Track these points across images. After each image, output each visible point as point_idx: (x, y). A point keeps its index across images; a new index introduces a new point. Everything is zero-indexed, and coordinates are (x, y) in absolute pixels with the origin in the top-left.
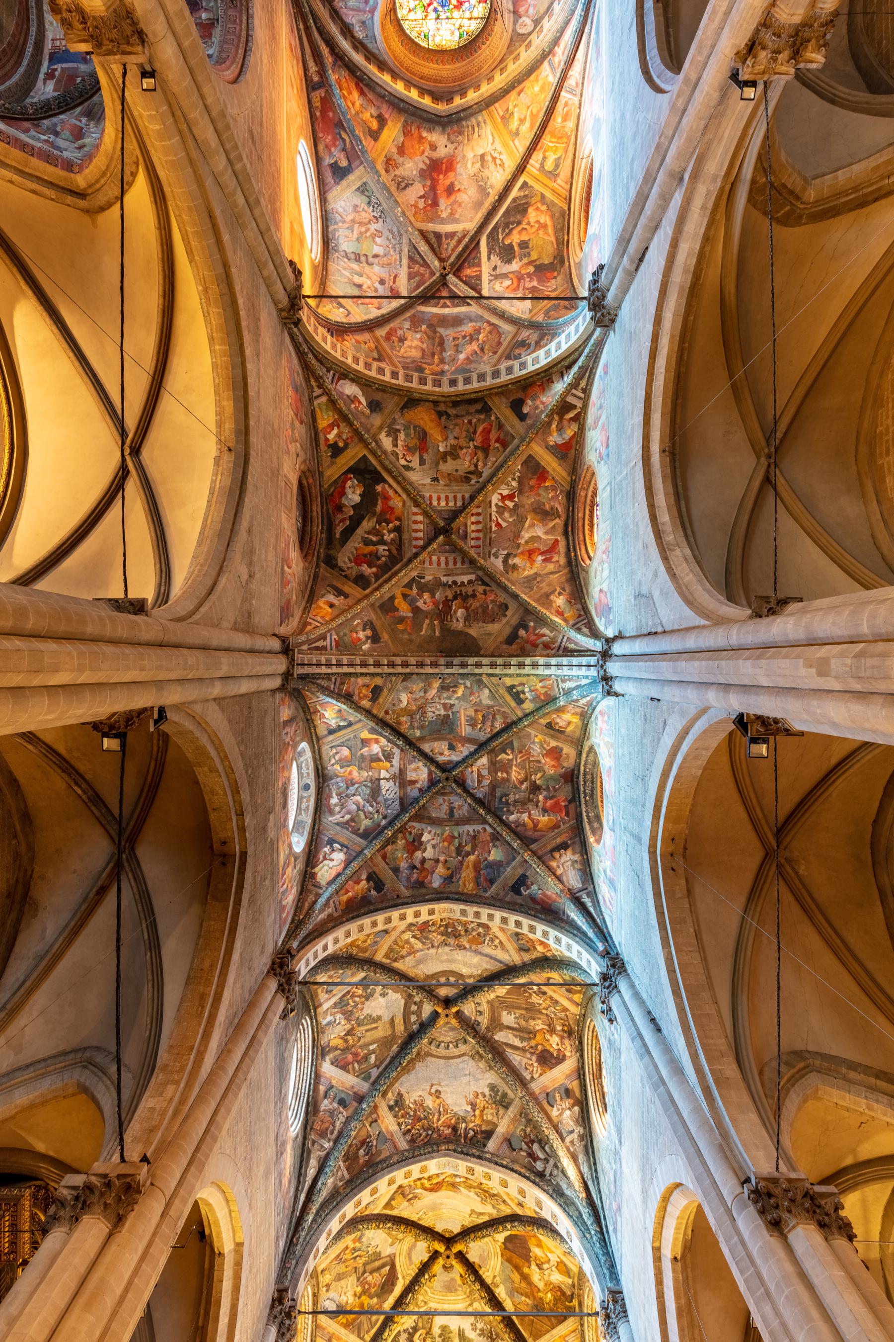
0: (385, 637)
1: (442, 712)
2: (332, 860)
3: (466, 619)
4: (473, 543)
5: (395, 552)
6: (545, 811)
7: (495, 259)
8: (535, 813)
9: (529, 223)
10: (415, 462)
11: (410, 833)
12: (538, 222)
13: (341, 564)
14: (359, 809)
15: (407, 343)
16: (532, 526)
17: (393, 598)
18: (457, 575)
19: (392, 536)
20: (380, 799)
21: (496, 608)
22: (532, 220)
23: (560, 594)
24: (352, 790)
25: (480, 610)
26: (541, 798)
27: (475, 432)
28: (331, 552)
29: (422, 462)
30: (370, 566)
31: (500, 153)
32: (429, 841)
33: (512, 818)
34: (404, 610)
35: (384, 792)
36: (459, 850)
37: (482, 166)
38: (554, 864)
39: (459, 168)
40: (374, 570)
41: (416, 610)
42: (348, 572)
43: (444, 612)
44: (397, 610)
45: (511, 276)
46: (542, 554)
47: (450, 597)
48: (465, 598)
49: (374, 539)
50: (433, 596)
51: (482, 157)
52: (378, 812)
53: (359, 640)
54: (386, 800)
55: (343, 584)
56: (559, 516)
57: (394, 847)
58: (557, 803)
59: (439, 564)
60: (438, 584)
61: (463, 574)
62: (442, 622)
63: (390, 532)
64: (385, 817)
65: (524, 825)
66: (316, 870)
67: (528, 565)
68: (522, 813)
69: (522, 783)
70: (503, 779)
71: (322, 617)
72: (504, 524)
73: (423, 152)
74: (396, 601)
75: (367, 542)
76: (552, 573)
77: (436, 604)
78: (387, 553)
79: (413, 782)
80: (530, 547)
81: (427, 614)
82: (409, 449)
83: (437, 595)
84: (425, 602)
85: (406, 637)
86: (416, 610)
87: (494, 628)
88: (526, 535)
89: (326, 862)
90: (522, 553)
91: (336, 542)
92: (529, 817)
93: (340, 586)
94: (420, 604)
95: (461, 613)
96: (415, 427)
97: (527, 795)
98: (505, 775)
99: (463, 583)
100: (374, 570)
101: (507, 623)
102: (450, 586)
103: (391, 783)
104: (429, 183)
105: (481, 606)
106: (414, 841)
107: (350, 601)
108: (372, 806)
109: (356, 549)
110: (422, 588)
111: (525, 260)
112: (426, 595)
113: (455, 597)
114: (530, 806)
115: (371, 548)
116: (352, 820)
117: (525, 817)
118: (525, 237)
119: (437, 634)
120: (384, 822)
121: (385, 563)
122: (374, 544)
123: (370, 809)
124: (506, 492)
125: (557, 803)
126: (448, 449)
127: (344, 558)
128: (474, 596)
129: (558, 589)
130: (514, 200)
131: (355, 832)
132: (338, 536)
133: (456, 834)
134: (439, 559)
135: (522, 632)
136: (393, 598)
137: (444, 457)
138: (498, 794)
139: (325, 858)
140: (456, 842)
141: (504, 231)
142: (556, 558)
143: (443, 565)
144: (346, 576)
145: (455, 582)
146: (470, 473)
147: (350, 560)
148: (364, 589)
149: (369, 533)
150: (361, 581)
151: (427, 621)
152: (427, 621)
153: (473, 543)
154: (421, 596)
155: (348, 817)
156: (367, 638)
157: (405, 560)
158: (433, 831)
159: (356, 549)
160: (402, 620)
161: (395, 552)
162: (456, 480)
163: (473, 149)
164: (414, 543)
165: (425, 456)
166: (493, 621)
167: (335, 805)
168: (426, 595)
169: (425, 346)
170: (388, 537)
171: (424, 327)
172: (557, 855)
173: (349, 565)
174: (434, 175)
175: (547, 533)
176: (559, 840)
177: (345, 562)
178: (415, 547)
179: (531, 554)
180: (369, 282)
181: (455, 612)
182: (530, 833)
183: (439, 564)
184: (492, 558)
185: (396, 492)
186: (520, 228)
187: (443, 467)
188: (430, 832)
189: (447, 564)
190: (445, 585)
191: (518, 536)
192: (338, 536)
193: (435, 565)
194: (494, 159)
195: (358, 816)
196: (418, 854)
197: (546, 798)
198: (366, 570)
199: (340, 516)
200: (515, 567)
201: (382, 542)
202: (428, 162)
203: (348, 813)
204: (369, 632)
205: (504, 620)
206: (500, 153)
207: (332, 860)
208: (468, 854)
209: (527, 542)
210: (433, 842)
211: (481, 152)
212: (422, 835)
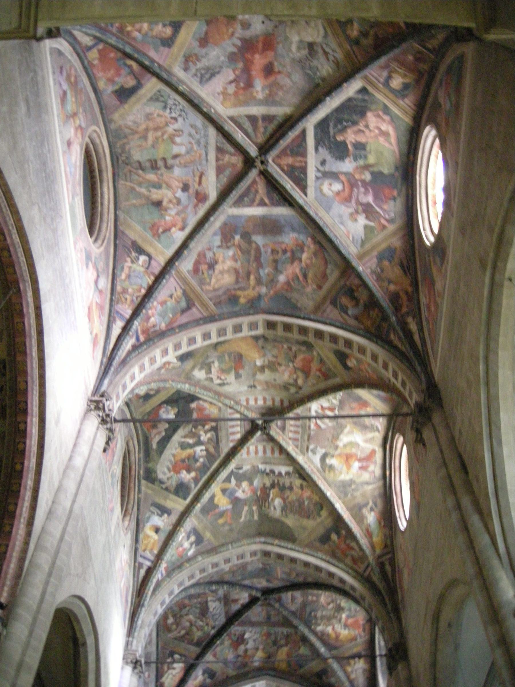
0: (208, 535)
1: (261, 566)
2: (174, 669)
3: (284, 509)
4: (291, 435)
5: (212, 450)
6: (346, 626)
7: (324, 152)
8: (339, 628)
9: (367, 126)
10: (231, 377)
11: (235, 635)
12: (379, 128)
13: (160, 476)
14: (191, 625)
15: (219, 267)
16: (351, 432)
17: (212, 498)
18: (275, 464)
19: (209, 435)
20: (209, 614)
21: (312, 506)
22: (372, 126)
23: (372, 509)
24: (185, 611)
25: (297, 504)
26: (344, 616)
27: (295, 357)
28: (150, 465)
29: (238, 376)
30: (189, 471)
31: (333, 51)
32: (250, 638)
33: (319, 628)
34: (223, 503)
35: (211, 609)
36: (275, 643)
37: (310, 54)
38: (349, 669)
39: (280, 48)
40: (193, 474)
41: (236, 502)
42: (168, 484)
43: (262, 499)
44: (217, 506)
45: (343, 178)
46: (360, 460)
47: (268, 484)
48: (282, 489)
49: (191, 441)
50: (251, 483)
51: (311, 46)
52: (207, 624)
53: (185, 550)
54: (213, 616)
55: (166, 498)
56: (378, 430)
57: (222, 646)
58: (356, 622)
59: (256, 452)
60: (256, 471)
61: (280, 464)
62: (260, 507)
63: (206, 432)
64: (213, 628)
65: (328, 635)
66: (164, 679)
67: (345, 468)
68: (327, 626)
69: (329, 604)
70: (312, 601)
71: (151, 551)
72: (323, 426)
73: (232, 35)
74: (216, 500)
75: (183, 446)
76: (367, 483)
77: (254, 492)
78: (204, 453)
79: (235, 601)
80: (348, 451)
81: (245, 502)
82: (223, 371)
83: (256, 483)
84: (244, 491)
85: (227, 528)
86: (236, 502)
87: (310, 524)
88: (344, 439)
89: (170, 671)
90: (340, 455)
91: (153, 454)
92: (333, 629)
93: (160, 501)
94: (240, 494)
95: (278, 502)
96: (230, 355)
97: (332, 613)
98: (315, 598)
99: (280, 474)
100: (193, 474)
101: (322, 522)
102: (267, 474)
103: (217, 604)
104: (240, 65)
105: (298, 500)
106: (238, 639)
107: (174, 518)
108: (202, 621)
109: (174, 456)
110: (240, 478)
111: (361, 162)
112: (245, 485)
113: (273, 486)
114: (334, 621)
115: (189, 451)
116: (187, 633)
117: (329, 629)
118: (361, 139)
119: (256, 518)
120: (213, 632)
121: (204, 465)
122: (191, 446)
123: (201, 623)
124: (326, 404)
125: (356, 622)
126: (266, 362)
127: (163, 469)
128: (291, 488)
129: (371, 504)
130: (350, 100)
131: (191, 642)
132: (154, 446)
133: (272, 632)
134: (256, 448)
135: (334, 537)
136: (212, 498)
137: (262, 369)
138: (308, 610)
139: (169, 668)
140: (273, 638)
141: (335, 126)
142: (371, 468)
143: (261, 453)
144: (167, 489)
145: (272, 472)
146: (290, 384)
147: (169, 470)
148: (185, 499)
149: (185, 437)
150: (181, 489)
151: (246, 508)
152: (246, 508)
153: (291, 435)
154: (239, 485)
155: (183, 632)
156: (191, 544)
157: (223, 455)
158: (253, 632)
159: (174, 456)
160: (222, 514)
161: (212, 450)
162: (274, 387)
163: (299, 34)
164: (231, 437)
165: (241, 372)
166: (308, 517)
167: (172, 624)
168: (245, 485)
169: (238, 265)
170: (204, 437)
171: (237, 238)
172: (352, 662)
173: (169, 475)
174: (249, 56)
175: (366, 441)
176: (355, 650)
177: (164, 473)
178: (232, 441)
179: (348, 458)
180: (169, 194)
181: (273, 500)
182: (332, 642)
183: (256, 452)
184: (310, 454)
185: (211, 403)
186: (355, 128)
187: (260, 377)
188: (251, 632)
189: (265, 452)
190: (263, 472)
191: (336, 437)
192: (154, 446)
193: (252, 454)
194: (326, 53)
195: (190, 630)
196: (242, 648)
197: (348, 617)
198: (186, 476)
199: (154, 431)
200: (331, 467)
201: (199, 443)
202: (239, 43)
203: (183, 628)
204: (193, 538)
205: (319, 520)
206: (333, 51)
207: (174, 669)
208: (281, 646)
209: (345, 446)
210: (254, 638)
211: (310, 39)
212: (244, 634)
